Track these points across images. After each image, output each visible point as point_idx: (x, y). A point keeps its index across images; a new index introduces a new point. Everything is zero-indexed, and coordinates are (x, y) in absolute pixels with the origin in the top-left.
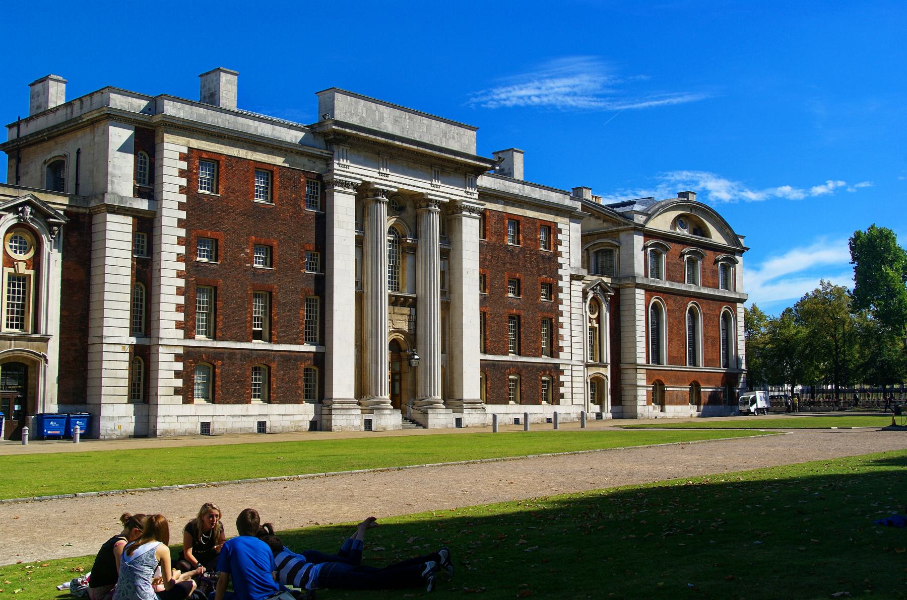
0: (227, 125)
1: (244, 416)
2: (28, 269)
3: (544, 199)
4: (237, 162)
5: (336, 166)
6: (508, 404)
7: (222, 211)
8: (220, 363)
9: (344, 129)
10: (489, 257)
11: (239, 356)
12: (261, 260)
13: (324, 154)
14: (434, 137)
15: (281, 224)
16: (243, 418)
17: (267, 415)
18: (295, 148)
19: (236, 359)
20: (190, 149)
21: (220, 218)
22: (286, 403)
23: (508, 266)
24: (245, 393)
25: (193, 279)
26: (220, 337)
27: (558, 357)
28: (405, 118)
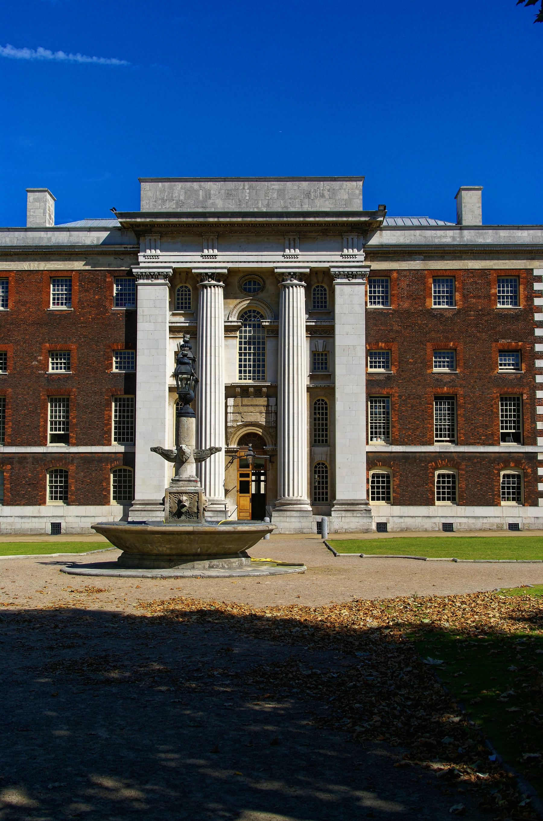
0: (15, 242)
1: (35, 517)
3: (502, 241)
4: (28, 275)
5: (141, 259)
6: (433, 504)
7: (11, 324)
8: (9, 467)
9: (133, 220)
10: (396, 327)
11: (30, 460)
12: (63, 366)
13: (129, 249)
14: (289, 201)
15: (81, 327)
16: (33, 519)
17: (63, 516)
18: (91, 249)
19: (27, 463)
21: (9, 331)
22: (87, 505)
23: (433, 335)
24: (37, 494)
26: (8, 443)
27: (534, 443)
28: (244, 188)
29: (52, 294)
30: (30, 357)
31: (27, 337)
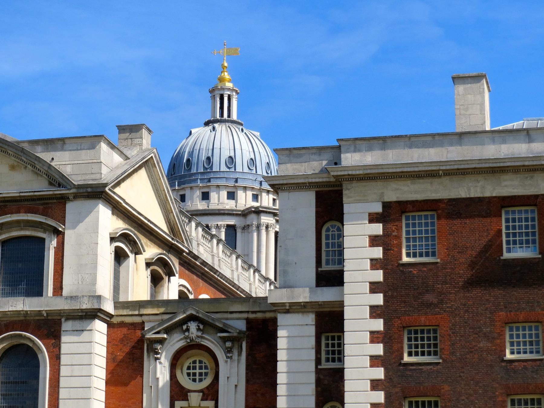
2: (206, 400)
20: (386, 205)
25: (397, 390)
29: (506, 233)
30: (477, 334)
31: (471, 303)
